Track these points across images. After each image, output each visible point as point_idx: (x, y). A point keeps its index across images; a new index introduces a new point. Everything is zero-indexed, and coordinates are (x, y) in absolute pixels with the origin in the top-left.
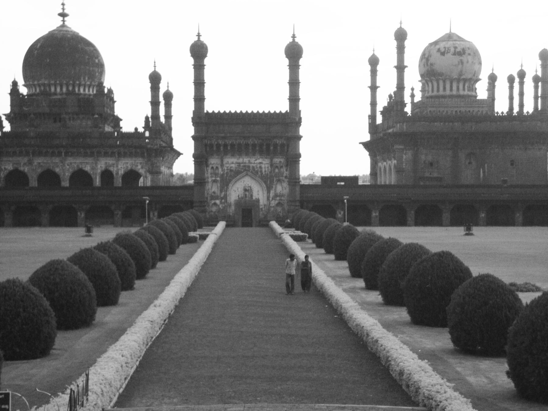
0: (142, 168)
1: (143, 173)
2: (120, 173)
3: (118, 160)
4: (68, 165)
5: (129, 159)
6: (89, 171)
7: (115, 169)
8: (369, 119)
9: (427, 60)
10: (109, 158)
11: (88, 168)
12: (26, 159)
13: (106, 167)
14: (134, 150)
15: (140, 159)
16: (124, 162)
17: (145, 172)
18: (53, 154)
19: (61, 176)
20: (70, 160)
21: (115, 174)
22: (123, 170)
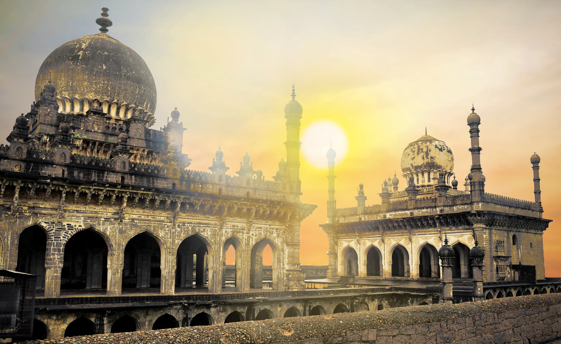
0: (278, 236)
1: (279, 244)
2: (251, 242)
4: (179, 226)
7: (245, 236)
8: (328, 204)
9: (427, 154)
10: (238, 219)
11: (207, 234)
13: (233, 232)
16: (256, 226)
20: (183, 218)
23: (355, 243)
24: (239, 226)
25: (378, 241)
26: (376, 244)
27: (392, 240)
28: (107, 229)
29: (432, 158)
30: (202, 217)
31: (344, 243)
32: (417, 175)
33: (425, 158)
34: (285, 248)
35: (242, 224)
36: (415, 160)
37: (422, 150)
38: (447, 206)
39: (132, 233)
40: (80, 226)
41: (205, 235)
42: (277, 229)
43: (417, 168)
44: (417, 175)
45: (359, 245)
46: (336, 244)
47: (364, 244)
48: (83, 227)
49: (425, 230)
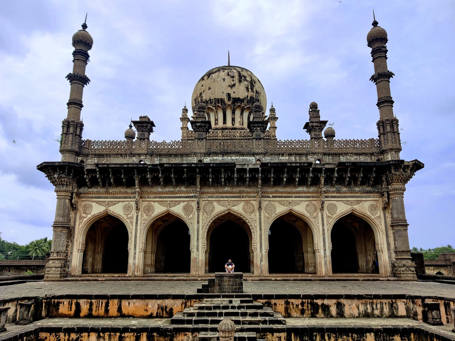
23: (127, 208)
25: (182, 204)
26: (178, 210)
27: (215, 203)
29: (257, 92)
31: (95, 207)
32: (233, 113)
33: (250, 90)
36: (234, 89)
37: (245, 77)
38: (329, 154)
43: (236, 100)
44: (233, 113)
45: (134, 213)
46: (74, 207)
47: (149, 209)
49: (288, 189)
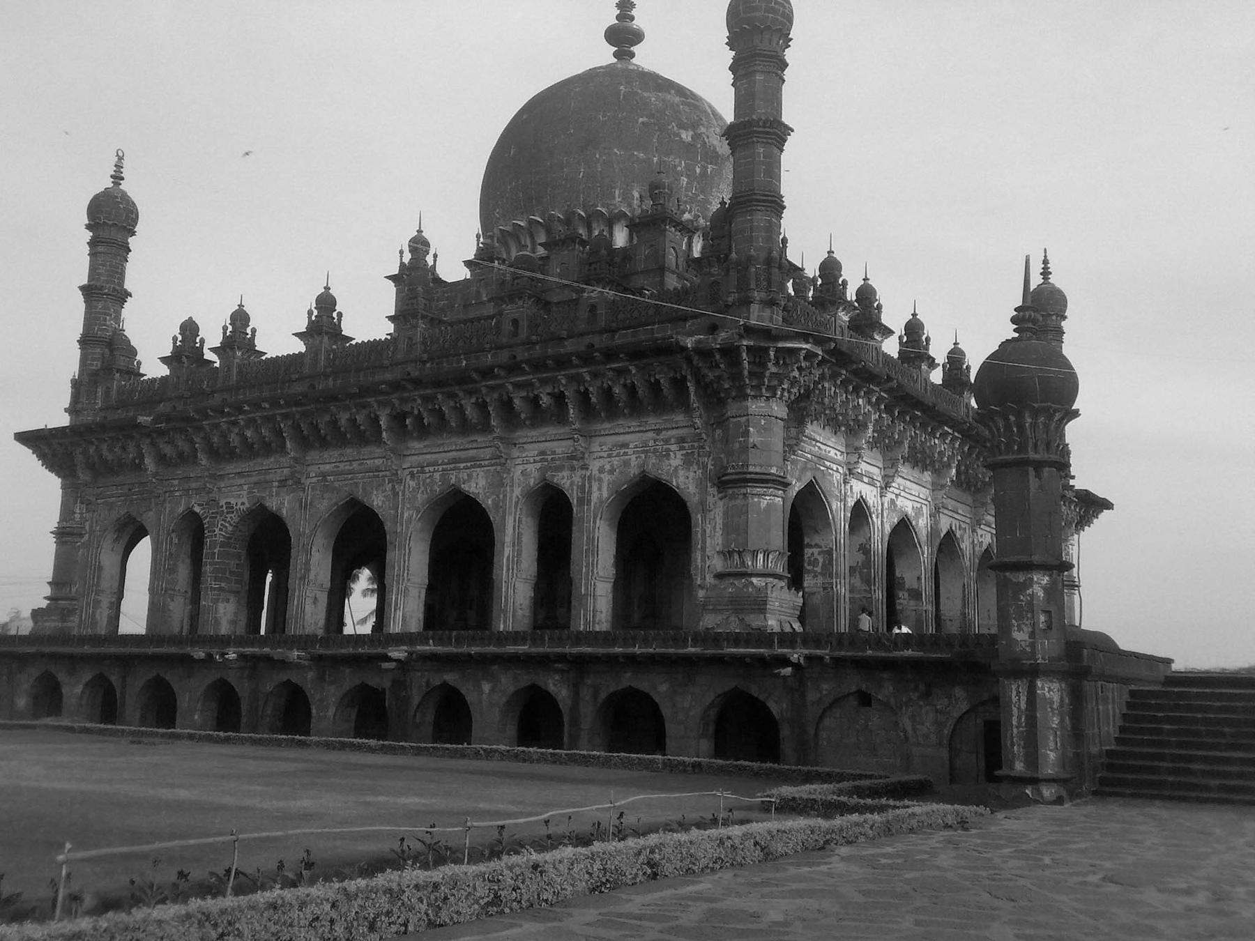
0: (687, 463)
2: (595, 496)
3: (589, 437)
4: (412, 474)
5: (633, 424)
6: (480, 499)
7: (577, 479)
11: (477, 485)
12: (277, 467)
13: (543, 470)
14: (635, 374)
15: (680, 418)
17: (700, 484)
18: (366, 436)
19: (388, 526)
20: (419, 451)
21: (574, 502)
22: (606, 477)
24: (559, 451)
28: (282, 503)
30: (460, 441)
34: (710, 500)
35: (564, 443)
39: (325, 505)
40: (243, 504)
41: (473, 490)
42: (681, 440)
48: (247, 505)
